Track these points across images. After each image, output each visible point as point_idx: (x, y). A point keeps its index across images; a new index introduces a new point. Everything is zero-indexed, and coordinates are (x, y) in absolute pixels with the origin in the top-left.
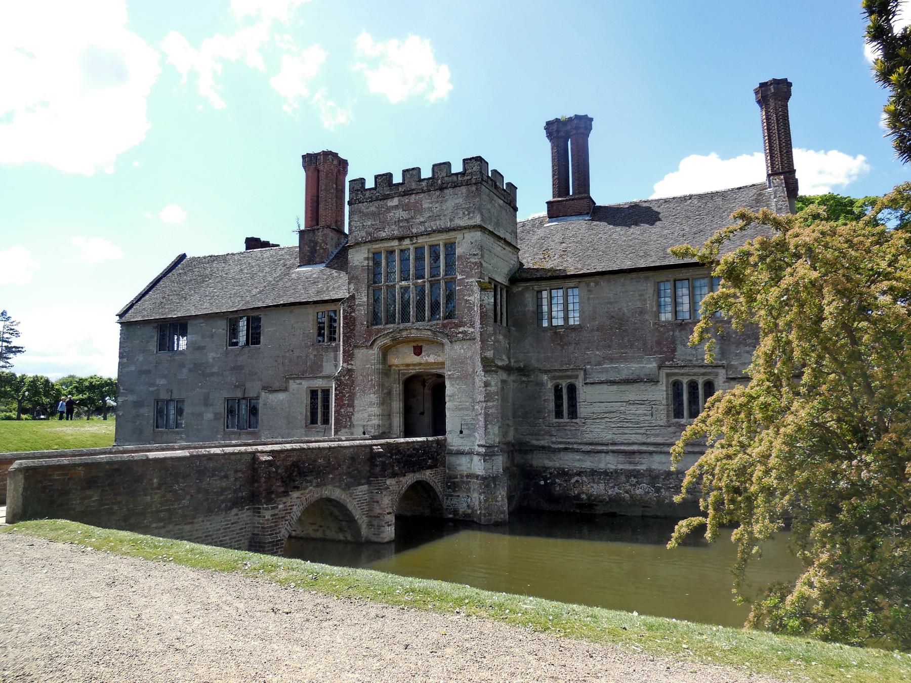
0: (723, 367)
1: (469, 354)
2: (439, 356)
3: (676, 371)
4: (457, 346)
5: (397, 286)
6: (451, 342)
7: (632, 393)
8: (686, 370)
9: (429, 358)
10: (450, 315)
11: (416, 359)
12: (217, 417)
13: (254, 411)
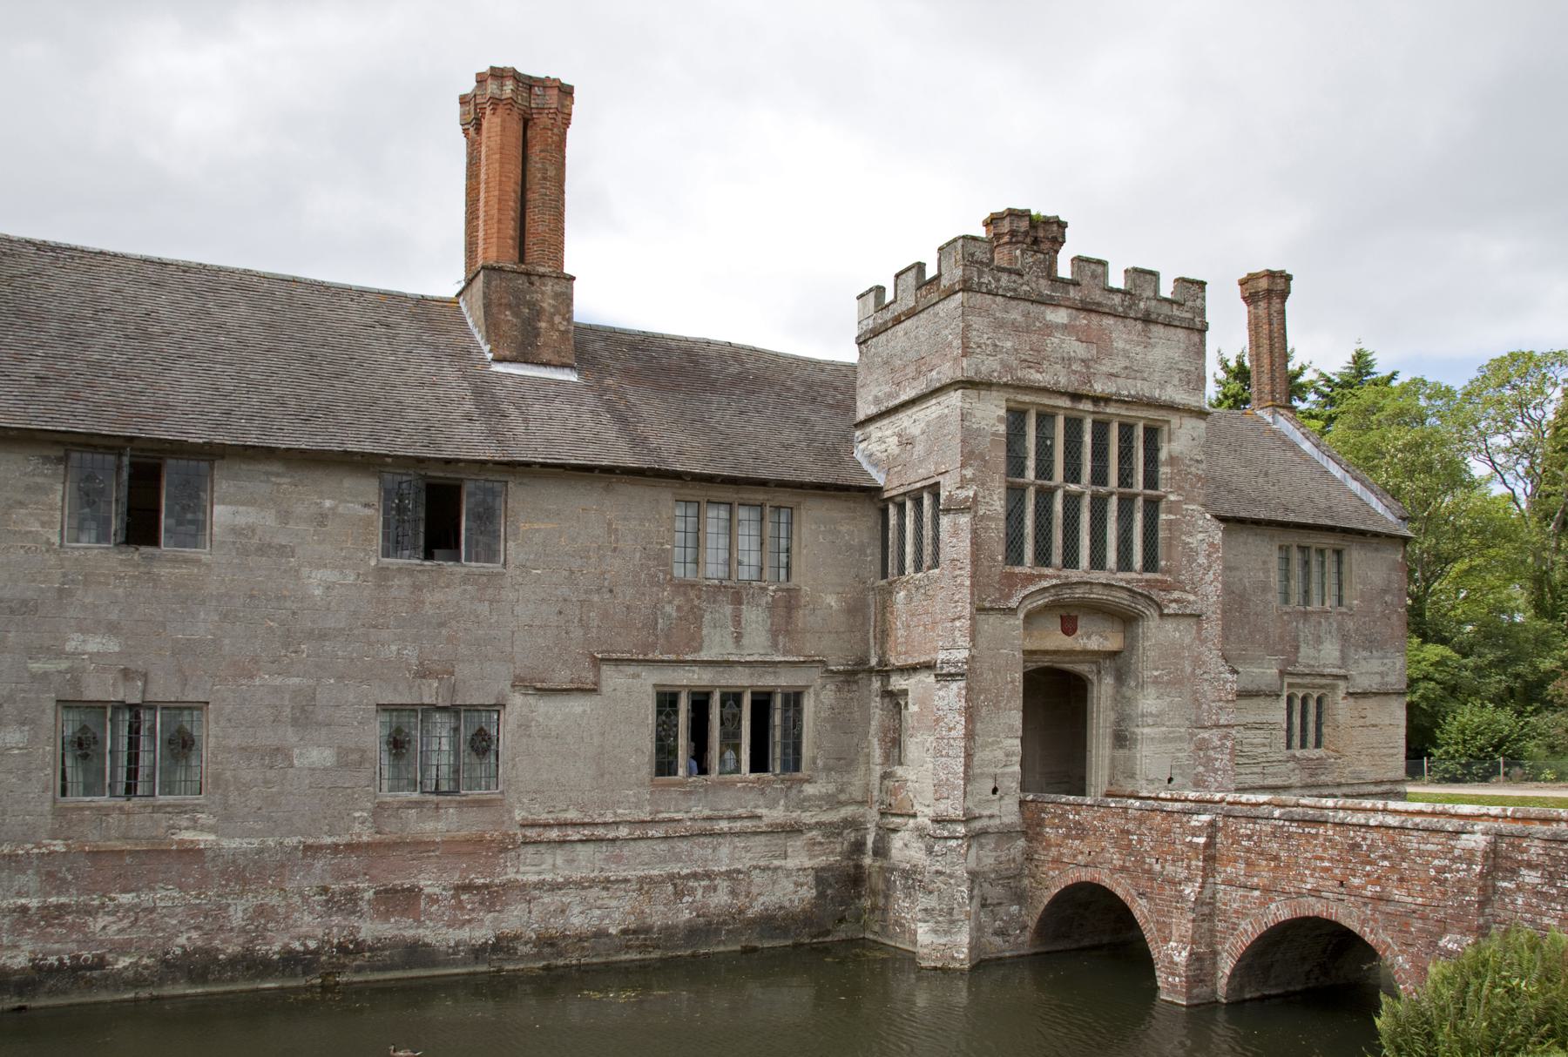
0: (1345, 677)
1: (1187, 641)
2: (1106, 638)
3: (1298, 680)
4: (1169, 625)
5: (1059, 496)
6: (1162, 615)
7: (1253, 712)
8: (1307, 680)
9: (1095, 638)
10: (1150, 563)
11: (1066, 642)
12: (349, 760)
13: (482, 744)
